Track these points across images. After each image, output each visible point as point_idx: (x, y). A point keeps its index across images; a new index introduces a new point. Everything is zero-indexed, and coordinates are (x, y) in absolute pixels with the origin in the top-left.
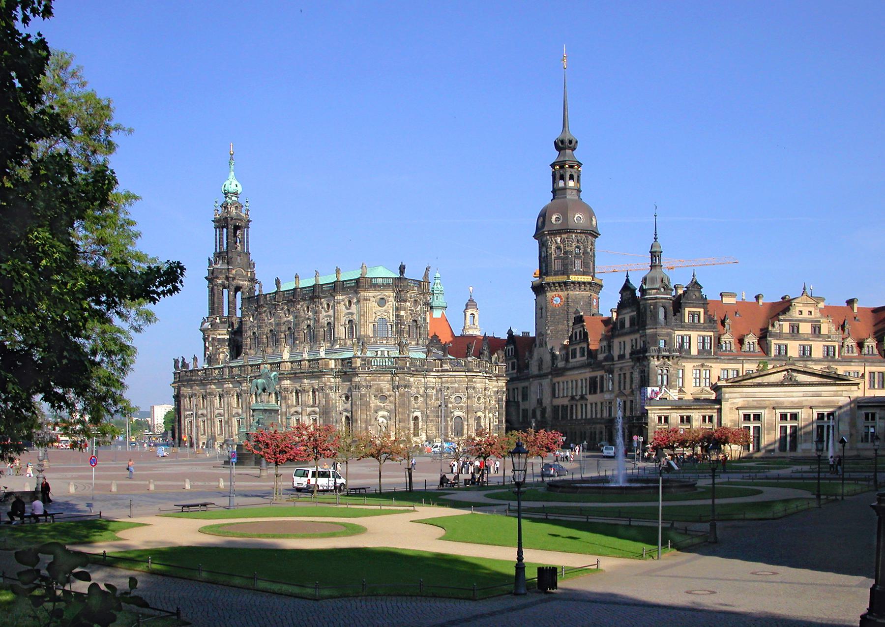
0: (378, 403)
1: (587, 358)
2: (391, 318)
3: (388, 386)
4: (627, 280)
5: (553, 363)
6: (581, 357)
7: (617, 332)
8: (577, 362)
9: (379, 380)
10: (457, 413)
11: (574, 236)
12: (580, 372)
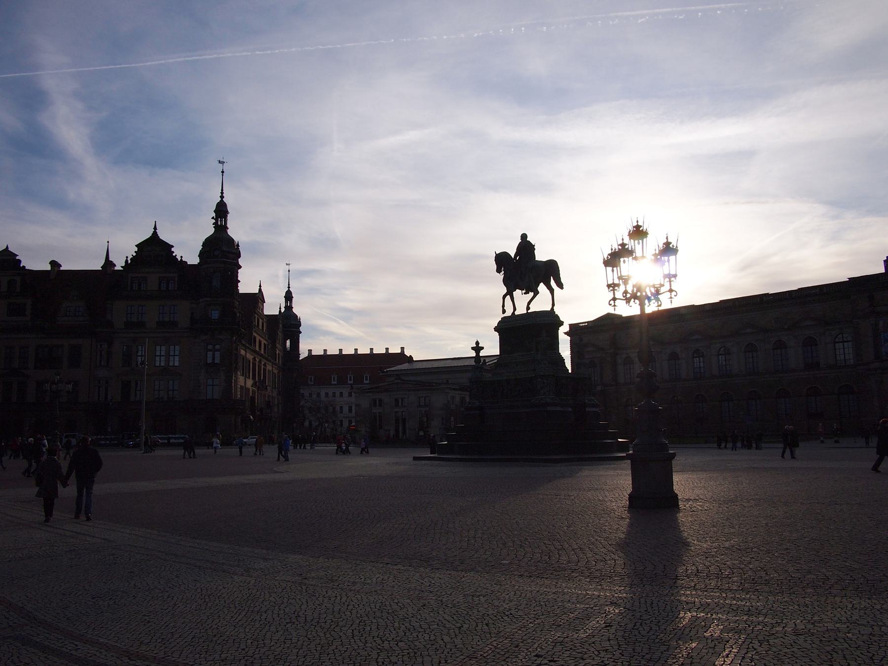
4: (155, 234)
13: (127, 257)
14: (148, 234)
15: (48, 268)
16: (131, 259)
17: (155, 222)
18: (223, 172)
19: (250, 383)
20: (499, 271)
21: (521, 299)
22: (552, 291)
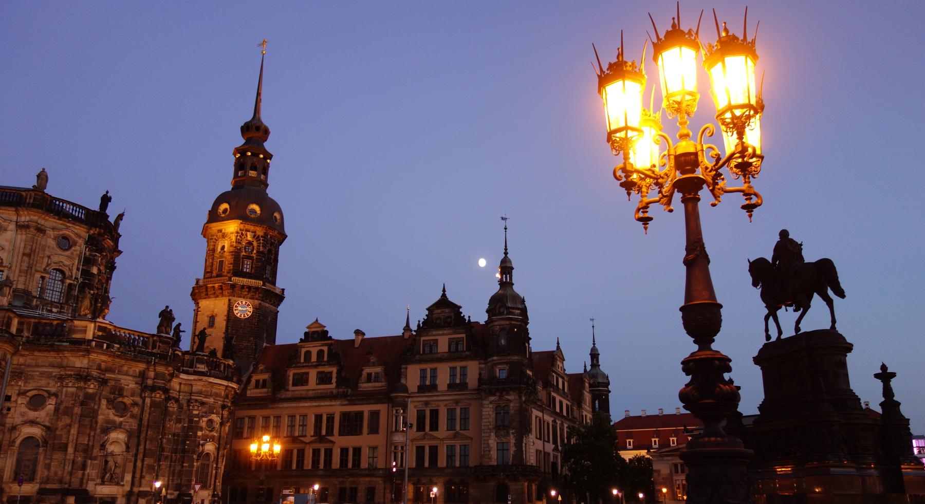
0: (111, 415)
1: (337, 387)
2: (74, 271)
3: (132, 385)
4: (444, 295)
6: (317, 384)
7: (417, 357)
9: (120, 372)
10: (210, 447)
11: (269, 237)
13: (419, 321)
14: (437, 297)
15: (352, 336)
16: (423, 323)
18: (506, 229)
19: (550, 447)
20: (755, 284)
21: (787, 316)
22: (830, 303)
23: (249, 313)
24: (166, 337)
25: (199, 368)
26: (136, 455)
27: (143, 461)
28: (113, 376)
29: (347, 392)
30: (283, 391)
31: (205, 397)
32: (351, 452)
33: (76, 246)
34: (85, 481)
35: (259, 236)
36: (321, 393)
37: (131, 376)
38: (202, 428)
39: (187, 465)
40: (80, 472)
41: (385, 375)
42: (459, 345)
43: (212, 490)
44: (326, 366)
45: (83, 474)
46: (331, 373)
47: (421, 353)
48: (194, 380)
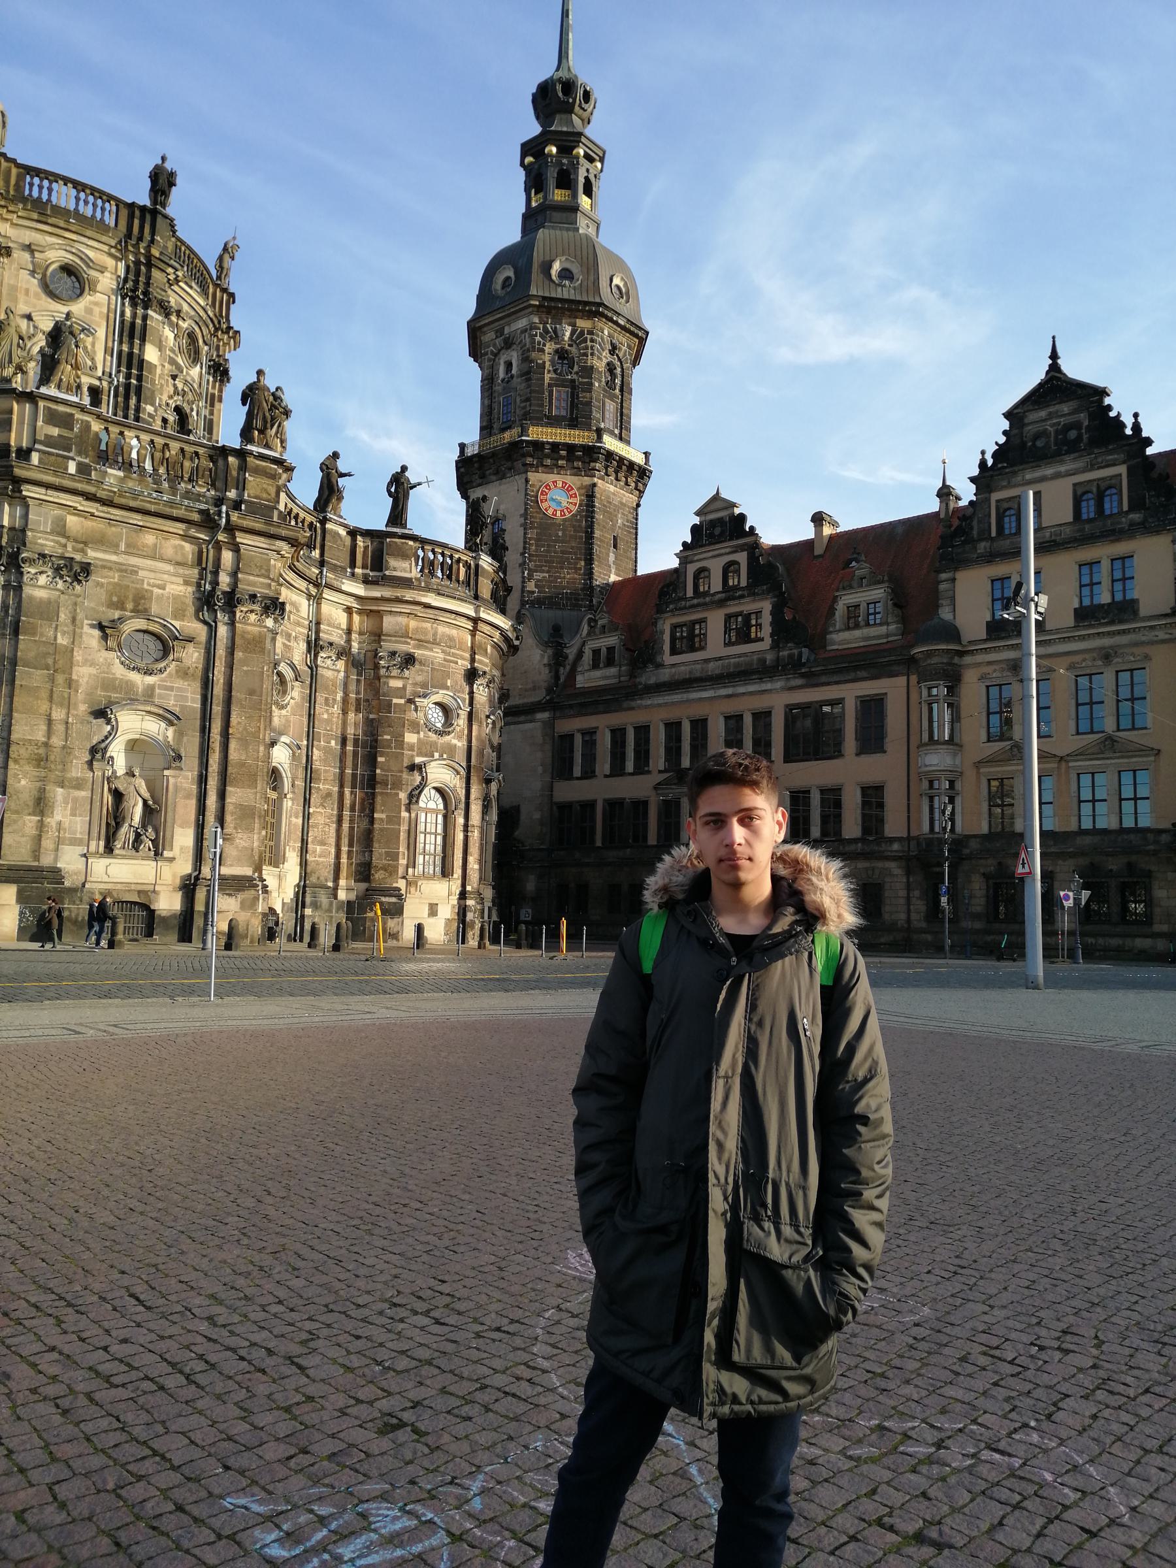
1: (775, 646)
4: (1054, 368)
5: (557, 677)
7: (982, 547)
8: (707, 661)
9: (133, 549)
12: (723, 692)
13: (983, 453)
14: (1037, 375)
15: (807, 532)
16: (995, 455)
17: (1054, 338)
23: (571, 507)
24: (262, 457)
25: (395, 569)
26: (202, 780)
27: (222, 796)
28: (114, 558)
29: (800, 655)
30: (650, 667)
31: (418, 647)
32: (816, 799)
33: (95, 291)
34: (47, 843)
35: (582, 333)
36: (737, 665)
37: (169, 561)
38: (418, 724)
39: (383, 816)
40: (31, 821)
41: (895, 605)
42: (1107, 499)
43: (459, 882)
44: (747, 600)
45: (41, 826)
46: (758, 613)
47: (994, 534)
48: (383, 599)
